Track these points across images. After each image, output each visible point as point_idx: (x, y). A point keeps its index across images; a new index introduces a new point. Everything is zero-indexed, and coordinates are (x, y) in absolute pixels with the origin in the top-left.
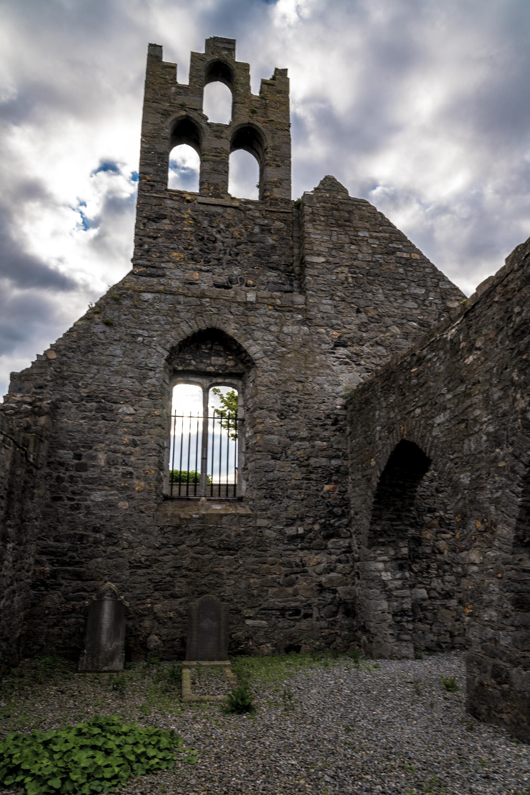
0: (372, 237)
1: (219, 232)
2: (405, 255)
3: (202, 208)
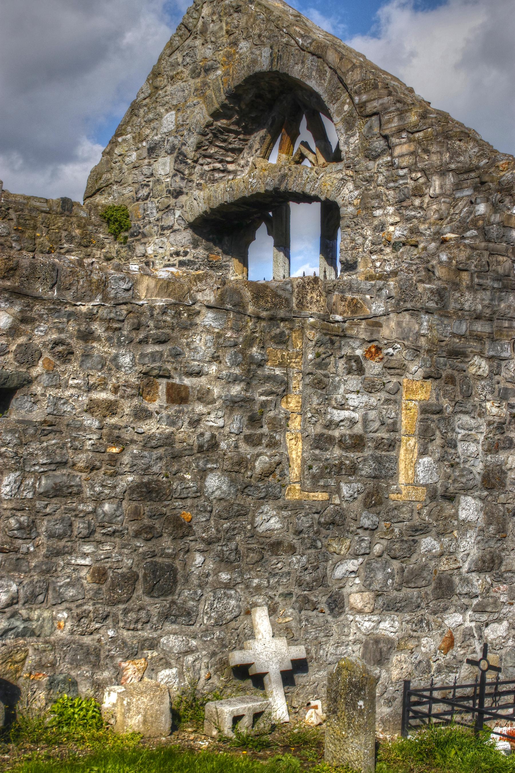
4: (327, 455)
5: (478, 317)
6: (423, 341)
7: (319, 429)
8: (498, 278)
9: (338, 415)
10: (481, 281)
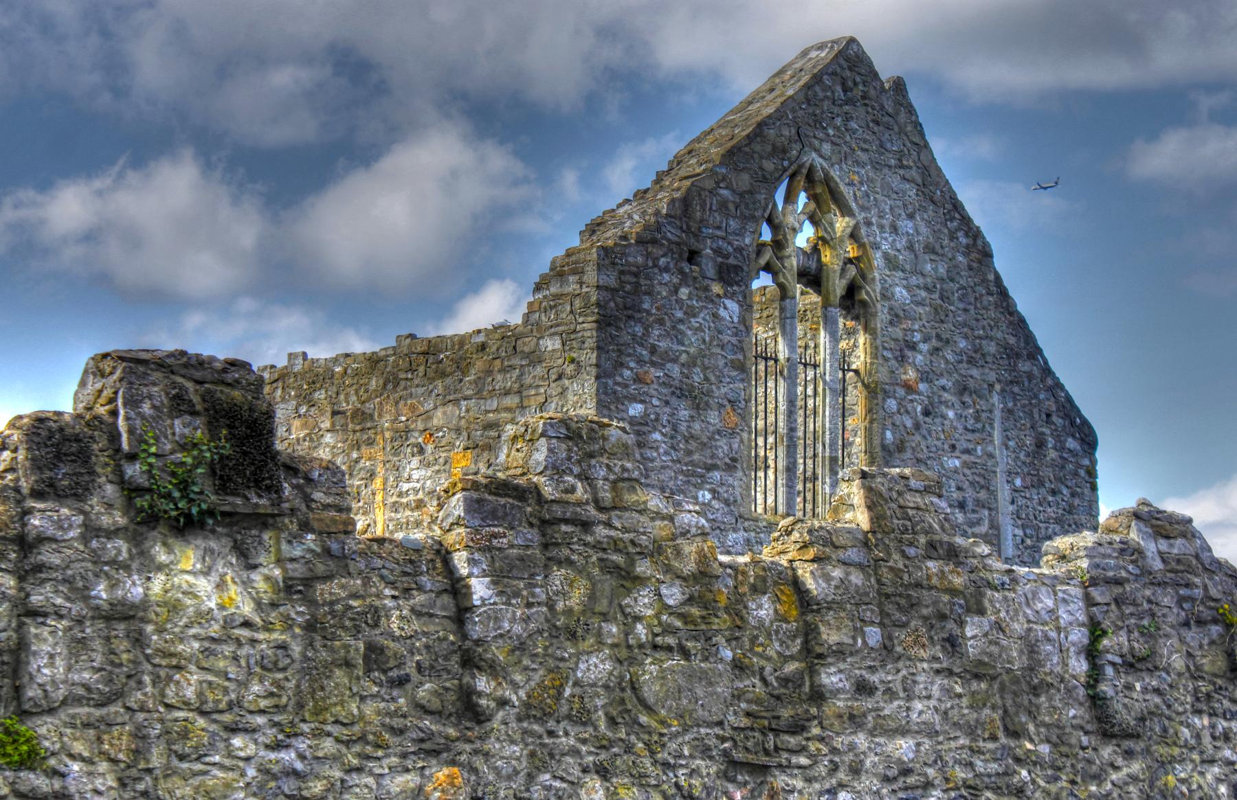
4: (399, 516)
5: (507, 393)
6: (463, 422)
7: (395, 499)
8: (527, 355)
10: (510, 363)
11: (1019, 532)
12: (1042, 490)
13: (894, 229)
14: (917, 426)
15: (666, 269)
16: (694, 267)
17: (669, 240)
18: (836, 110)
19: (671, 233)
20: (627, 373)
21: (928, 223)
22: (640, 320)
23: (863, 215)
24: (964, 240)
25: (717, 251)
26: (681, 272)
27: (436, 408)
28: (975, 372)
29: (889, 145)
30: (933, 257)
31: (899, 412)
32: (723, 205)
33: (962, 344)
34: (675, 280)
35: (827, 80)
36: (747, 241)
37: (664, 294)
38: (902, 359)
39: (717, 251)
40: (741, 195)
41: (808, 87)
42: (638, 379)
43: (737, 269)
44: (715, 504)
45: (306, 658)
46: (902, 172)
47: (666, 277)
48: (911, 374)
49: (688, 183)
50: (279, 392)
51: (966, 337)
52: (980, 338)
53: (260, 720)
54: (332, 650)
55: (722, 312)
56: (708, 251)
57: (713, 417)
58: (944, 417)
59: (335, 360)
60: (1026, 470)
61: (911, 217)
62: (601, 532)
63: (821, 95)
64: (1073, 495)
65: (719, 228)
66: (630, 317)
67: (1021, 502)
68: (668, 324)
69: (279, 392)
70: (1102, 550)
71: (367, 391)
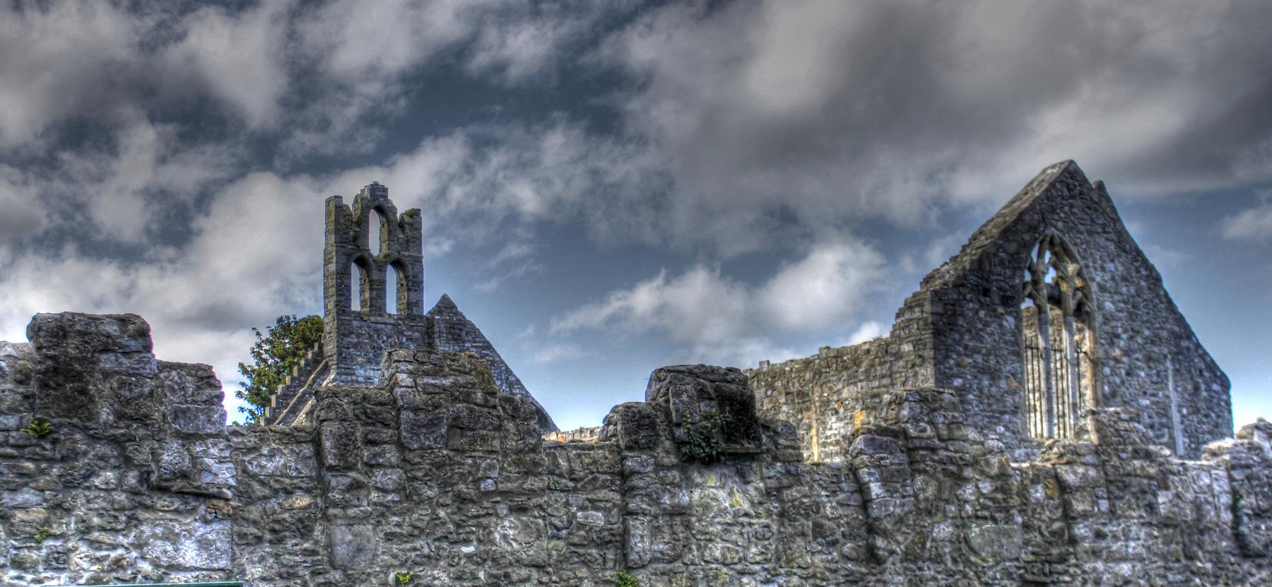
0: (472, 346)
1: (383, 342)
2: (491, 359)
3: (373, 325)
4: (826, 450)
5: (884, 376)
6: (859, 395)
7: (823, 440)
9: (829, 433)
11: (1187, 440)
12: (1200, 416)
13: (1103, 269)
14: (1123, 382)
15: (971, 301)
16: (987, 299)
17: (971, 284)
18: (1064, 202)
19: (973, 279)
20: (952, 362)
21: (1123, 264)
22: (957, 331)
23: (1084, 262)
24: (1144, 272)
25: (1000, 289)
26: (979, 301)
27: (843, 387)
28: (1156, 349)
29: (1097, 221)
30: (1127, 283)
31: (1112, 375)
32: (1002, 262)
33: (1147, 333)
34: (977, 307)
35: (1058, 185)
36: (1017, 281)
37: (971, 315)
38: (1112, 344)
39: (1000, 289)
40: (1012, 255)
41: (1047, 190)
42: (958, 365)
43: (1012, 298)
44: (1007, 434)
45: (780, 532)
46: (1105, 235)
47: (971, 305)
48: (1117, 352)
49: (980, 250)
50: (755, 383)
51: (1149, 329)
52: (1157, 329)
53: (757, 567)
54: (794, 527)
55: (1005, 323)
56: (995, 289)
57: (1003, 384)
58: (1138, 376)
59: (786, 364)
60: (1189, 404)
61: (1112, 261)
62: (943, 453)
63: (1055, 194)
64: (1218, 416)
65: (1000, 275)
66: (951, 330)
67: (1187, 422)
68: (974, 332)
69: (755, 383)
70: (1237, 448)
71: (804, 380)
